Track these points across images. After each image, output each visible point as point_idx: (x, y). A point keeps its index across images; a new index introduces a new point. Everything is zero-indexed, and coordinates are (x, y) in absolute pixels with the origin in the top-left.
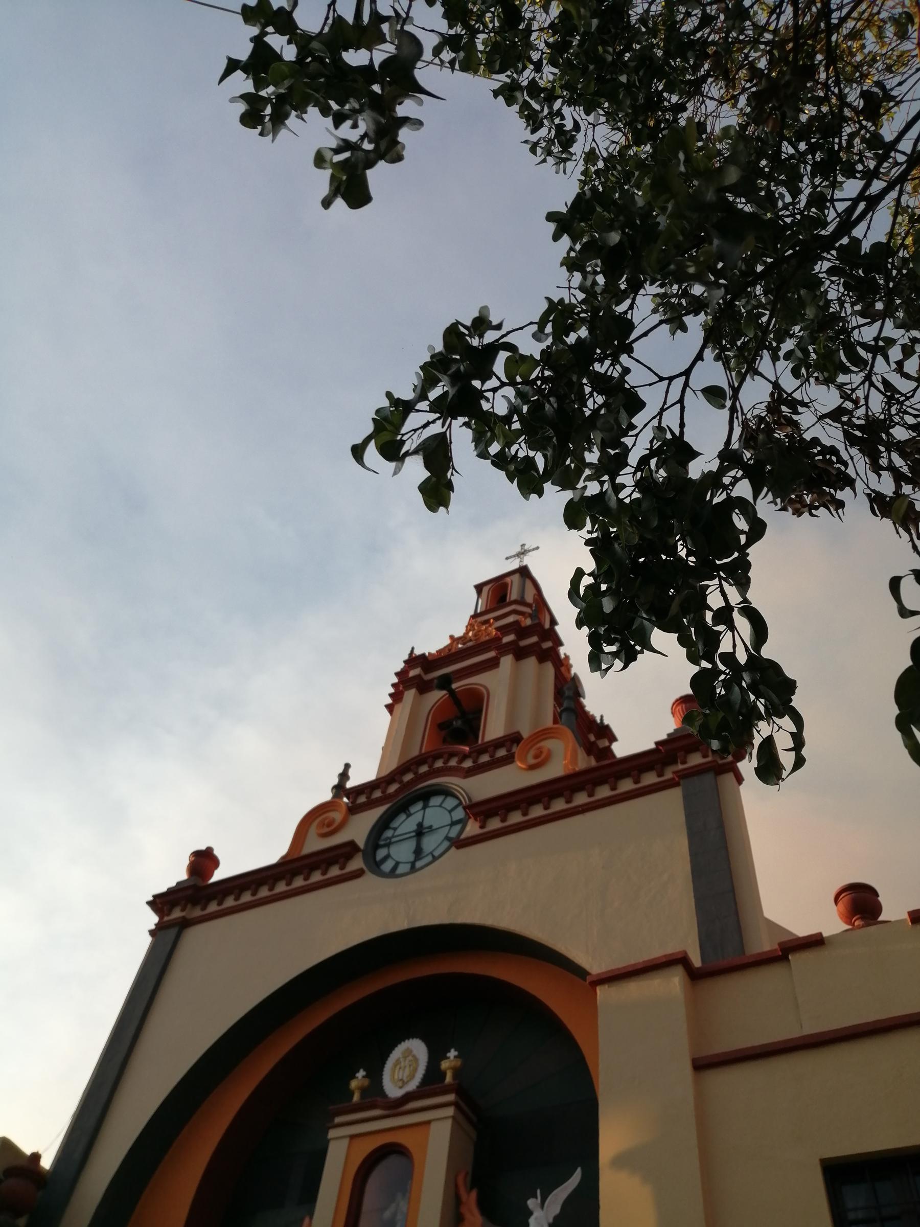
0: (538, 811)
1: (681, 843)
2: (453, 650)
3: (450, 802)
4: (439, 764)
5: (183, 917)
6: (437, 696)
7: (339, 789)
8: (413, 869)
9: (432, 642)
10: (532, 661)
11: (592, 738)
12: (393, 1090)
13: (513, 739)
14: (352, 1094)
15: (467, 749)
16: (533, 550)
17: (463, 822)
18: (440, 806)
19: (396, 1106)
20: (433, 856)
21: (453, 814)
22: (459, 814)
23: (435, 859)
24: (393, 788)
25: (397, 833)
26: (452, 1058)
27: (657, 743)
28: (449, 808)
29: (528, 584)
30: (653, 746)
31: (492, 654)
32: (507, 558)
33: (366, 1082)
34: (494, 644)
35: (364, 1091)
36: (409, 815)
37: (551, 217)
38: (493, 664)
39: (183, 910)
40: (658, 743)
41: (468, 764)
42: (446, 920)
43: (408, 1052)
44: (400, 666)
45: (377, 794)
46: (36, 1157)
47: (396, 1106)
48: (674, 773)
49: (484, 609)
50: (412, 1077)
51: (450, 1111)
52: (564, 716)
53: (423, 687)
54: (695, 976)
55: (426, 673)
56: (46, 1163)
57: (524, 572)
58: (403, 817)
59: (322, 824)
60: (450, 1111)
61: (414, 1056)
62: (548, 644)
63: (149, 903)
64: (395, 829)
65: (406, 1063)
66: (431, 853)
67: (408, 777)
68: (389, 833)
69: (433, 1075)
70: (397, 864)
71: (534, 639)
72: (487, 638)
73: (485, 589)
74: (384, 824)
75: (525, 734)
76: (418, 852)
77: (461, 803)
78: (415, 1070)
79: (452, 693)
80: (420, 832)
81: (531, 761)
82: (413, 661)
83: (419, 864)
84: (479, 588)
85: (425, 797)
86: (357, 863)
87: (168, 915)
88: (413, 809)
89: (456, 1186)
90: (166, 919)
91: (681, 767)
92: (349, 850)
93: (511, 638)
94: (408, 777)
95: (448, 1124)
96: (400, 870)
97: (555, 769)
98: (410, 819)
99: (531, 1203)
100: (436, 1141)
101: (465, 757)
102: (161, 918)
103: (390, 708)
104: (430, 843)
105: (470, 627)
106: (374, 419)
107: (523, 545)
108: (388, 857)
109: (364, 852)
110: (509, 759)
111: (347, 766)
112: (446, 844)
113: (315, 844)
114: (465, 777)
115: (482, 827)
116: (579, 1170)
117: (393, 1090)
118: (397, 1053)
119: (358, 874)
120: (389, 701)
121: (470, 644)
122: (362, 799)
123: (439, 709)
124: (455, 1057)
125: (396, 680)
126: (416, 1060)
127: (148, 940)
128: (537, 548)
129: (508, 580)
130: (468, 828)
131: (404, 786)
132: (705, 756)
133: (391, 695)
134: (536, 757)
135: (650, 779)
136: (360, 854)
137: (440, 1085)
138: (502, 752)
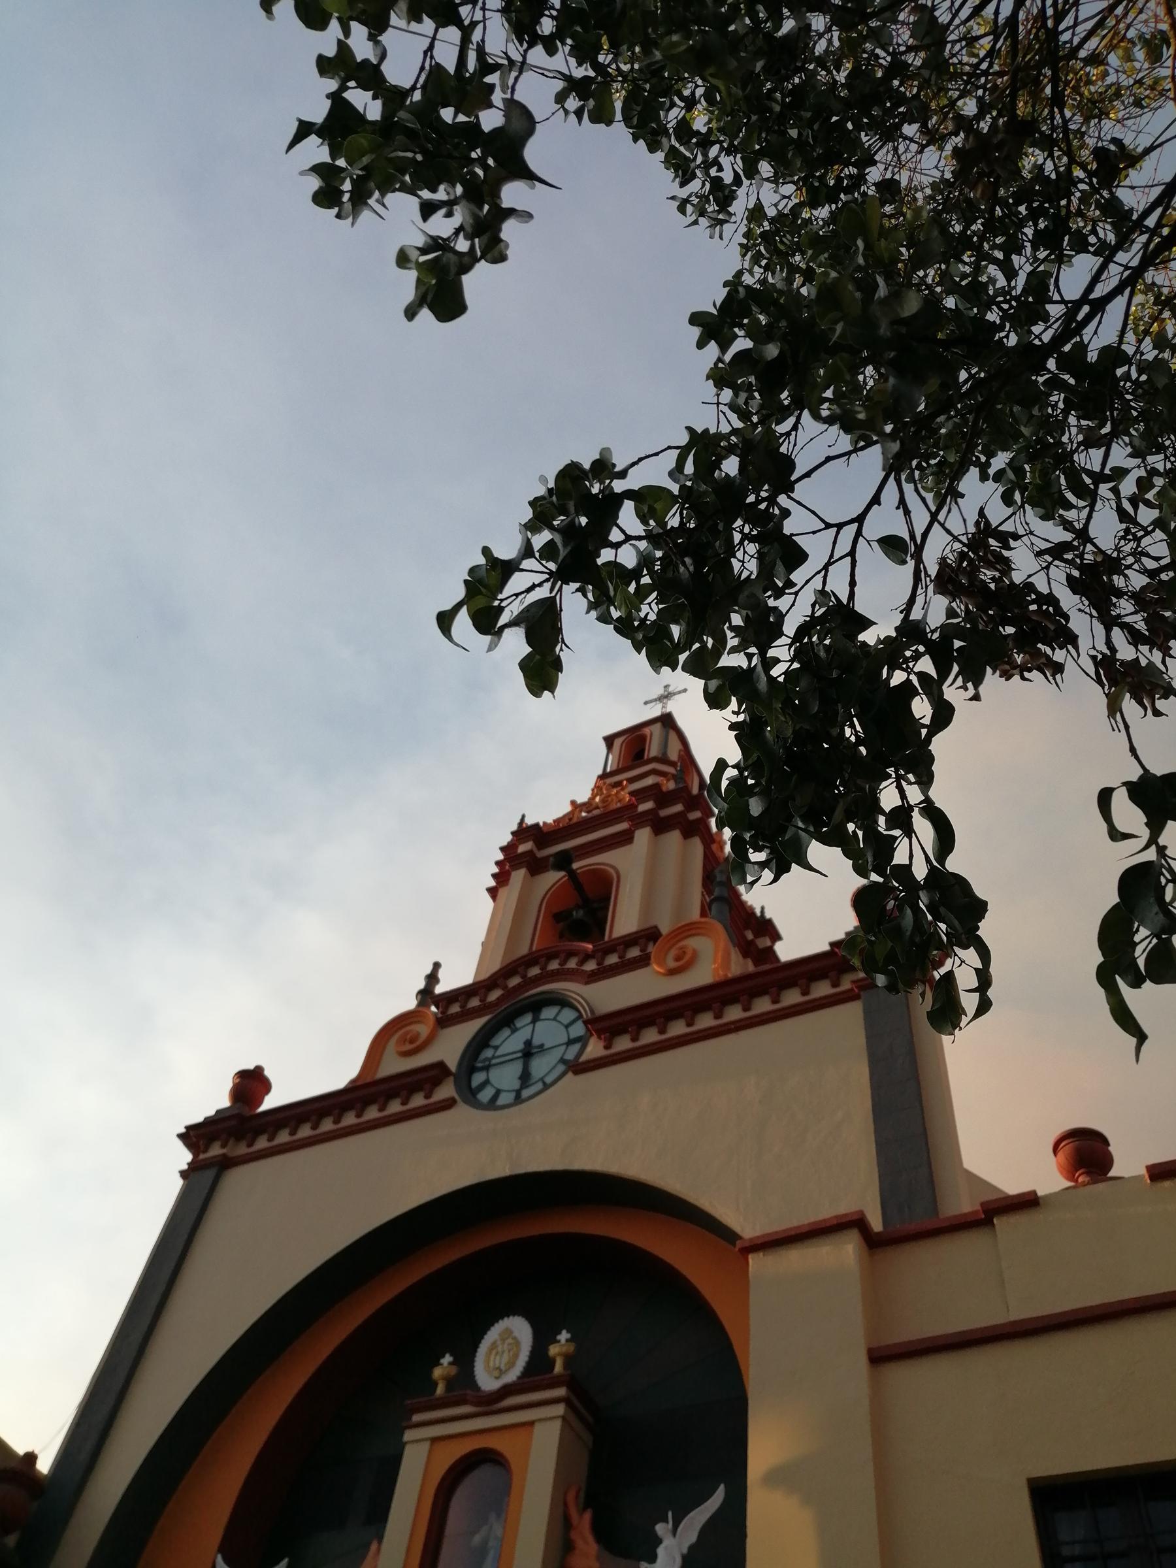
1: (860, 1072)
2: (575, 820)
3: (568, 1015)
4: (554, 965)
5: (224, 1155)
6: (552, 878)
7: (426, 995)
8: (518, 1099)
9: (548, 810)
10: (675, 836)
11: (750, 935)
12: (487, 1382)
13: (650, 935)
14: (436, 1384)
15: (590, 946)
16: (680, 692)
17: (583, 1041)
18: (555, 1019)
19: (490, 1402)
20: (544, 1083)
21: (571, 1029)
22: (578, 1030)
23: (546, 1087)
24: (494, 996)
25: (499, 1053)
26: (563, 1341)
27: (832, 944)
28: (566, 1022)
29: (673, 736)
30: (827, 948)
31: (624, 826)
32: (646, 703)
33: (454, 1370)
35: (450, 1382)
37: (696, 319)
38: (625, 839)
39: (223, 1146)
40: (833, 944)
41: (591, 966)
42: (559, 1166)
43: (508, 1332)
44: (507, 838)
45: (474, 1002)
46: (31, 1458)
47: (490, 1402)
48: (853, 982)
49: (615, 768)
50: (511, 1364)
51: (560, 1409)
52: (714, 907)
53: (536, 867)
54: (874, 1243)
55: (540, 848)
56: (44, 1465)
57: (667, 720)
58: (506, 1032)
59: (403, 1040)
60: (560, 1409)
61: (515, 1338)
62: (696, 815)
63: (180, 1136)
64: (496, 1048)
65: (505, 1348)
66: (542, 1079)
67: (514, 981)
68: (488, 1053)
69: (538, 1364)
70: (498, 1092)
71: (679, 808)
72: (619, 805)
73: (618, 743)
74: (481, 1041)
75: (665, 929)
76: (525, 1078)
77: (580, 1016)
78: (516, 1356)
79: (572, 874)
80: (528, 1052)
81: (672, 964)
82: (524, 832)
83: (525, 1093)
84: (609, 740)
85: (535, 1007)
86: (446, 1090)
87: (205, 1151)
88: (519, 1023)
89: (566, 1505)
90: (202, 1156)
92: (438, 1072)
93: (648, 805)
94: (514, 981)
95: (557, 1425)
96: (504, 1099)
97: (702, 975)
98: (516, 1034)
99: (660, 1528)
100: (541, 1447)
101: (587, 957)
102: (195, 1155)
103: (493, 892)
104: (540, 1066)
105: (597, 789)
106: (466, 581)
107: (666, 687)
108: (487, 1082)
109: (457, 1077)
110: (643, 961)
111: (437, 966)
112: (561, 1068)
113: (393, 1065)
114: (587, 983)
115: (607, 1047)
116: (722, 1487)
117: (487, 1382)
118: (493, 1334)
119: (448, 1104)
120: (492, 883)
121: (596, 812)
122: (455, 1009)
123: (555, 895)
124: (567, 1341)
125: (500, 857)
126: (517, 1343)
127: (179, 1183)
128: (685, 690)
129: (647, 731)
130: (589, 1049)
131: (510, 993)
133: (494, 876)
134: (677, 959)
135: (822, 989)
136: (452, 1078)
137: (547, 1376)
138: (634, 952)
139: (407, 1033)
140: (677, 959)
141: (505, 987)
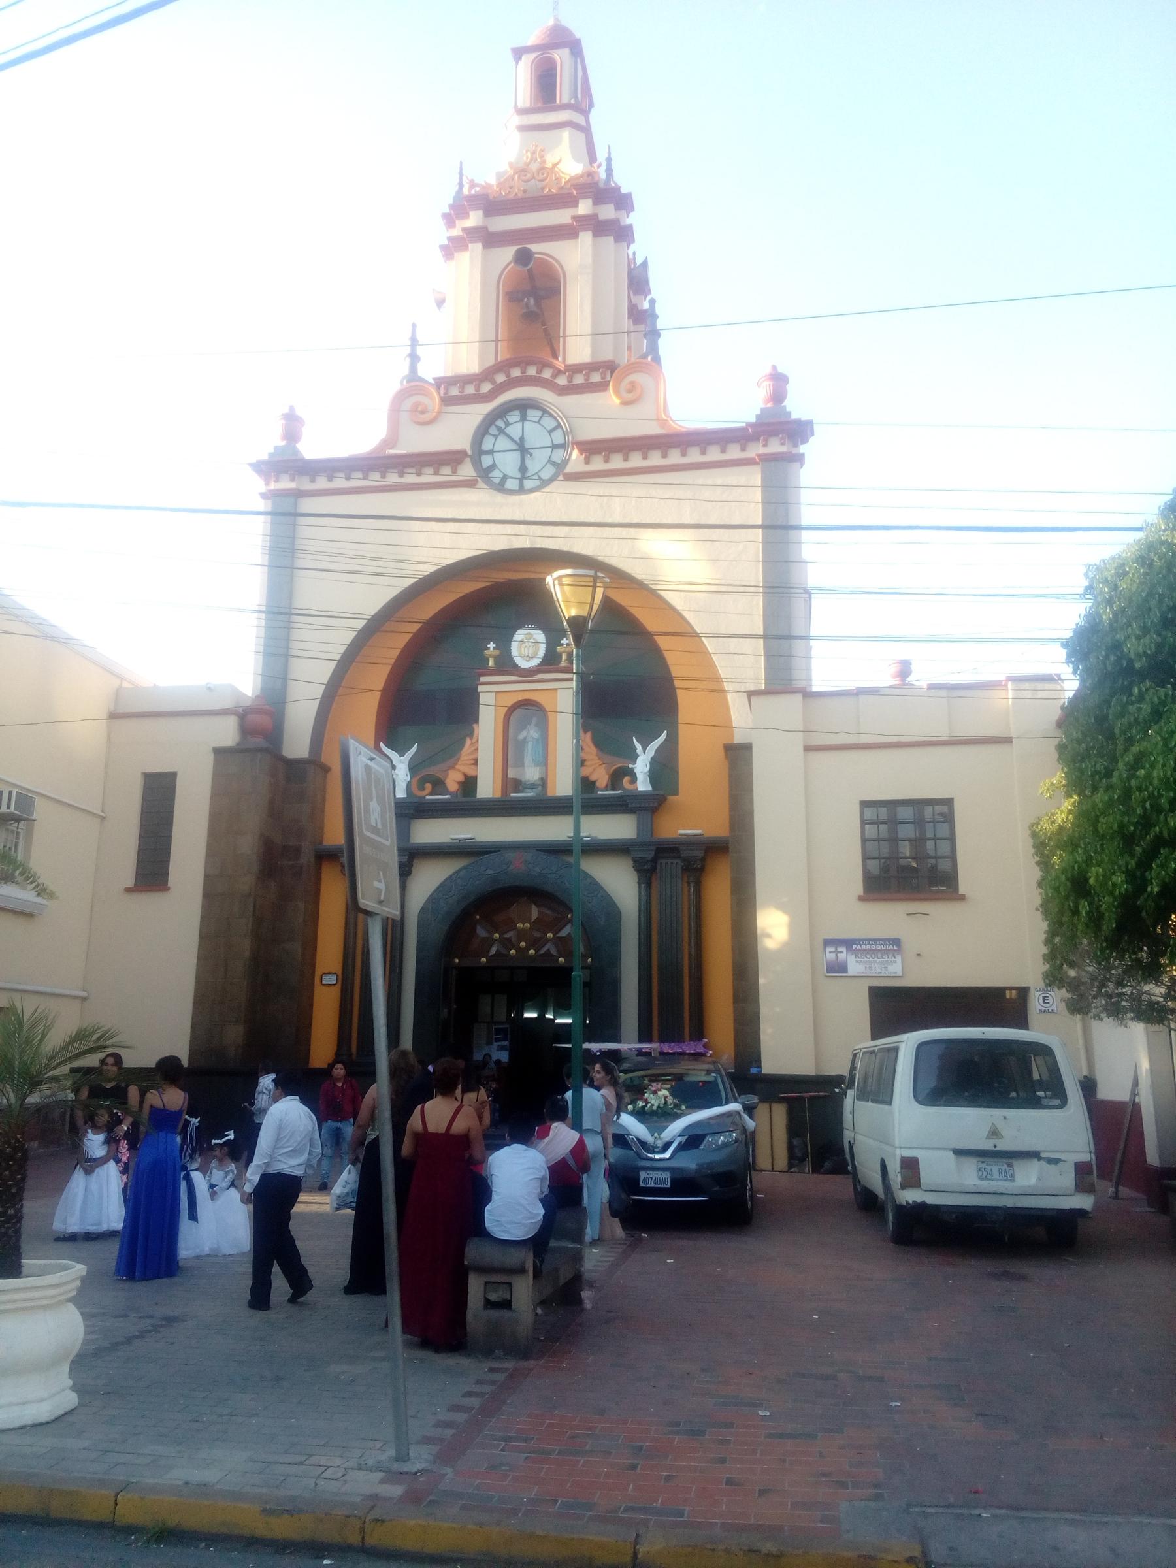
0: (636, 461)
3: (549, 423)
4: (532, 371)
10: (611, 239)
12: (523, 664)
18: (538, 422)
20: (540, 478)
23: (544, 483)
24: (486, 387)
33: (497, 652)
34: (563, 199)
35: (496, 658)
36: (508, 424)
39: (293, 480)
45: (470, 390)
63: (250, 465)
67: (500, 378)
70: (505, 478)
74: (482, 431)
76: (523, 469)
77: (559, 426)
80: (523, 449)
83: (528, 484)
86: (467, 470)
91: (762, 450)
94: (500, 378)
96: (511, 484)
102: (267, 484)
108: (493, 467)
110: (602, 387)
111: (414, 326)
115: (587, 461)
118: (520, 635)
119: (470, 484)
120: (446, 242)
132: (783, 444)
135: (734, 452)
136: (468, 460)
138: (596, 377)
139: (417, 404)
140: (630, 391)
141: (493, 382)
